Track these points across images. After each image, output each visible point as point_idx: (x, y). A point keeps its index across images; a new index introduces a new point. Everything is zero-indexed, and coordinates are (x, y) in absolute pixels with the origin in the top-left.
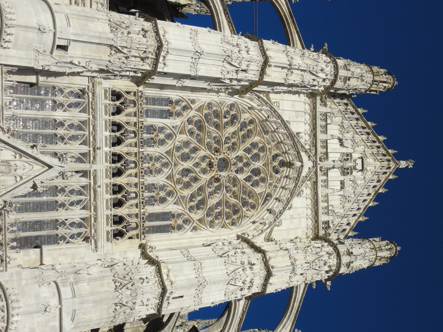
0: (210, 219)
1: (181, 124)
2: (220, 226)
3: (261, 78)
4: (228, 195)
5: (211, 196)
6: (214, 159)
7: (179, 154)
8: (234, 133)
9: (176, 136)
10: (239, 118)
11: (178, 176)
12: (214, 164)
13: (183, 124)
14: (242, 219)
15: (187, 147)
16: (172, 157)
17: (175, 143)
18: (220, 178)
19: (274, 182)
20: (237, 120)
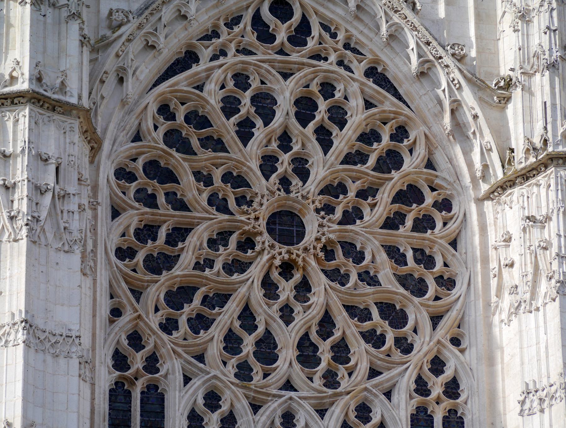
0: (432, 288)
1: (179, 355)
2: (453, 255)
3: (74, 112)
4: (366, 211)
5: (372, 274)
6: (273, 257)
7: (257, 368)
8: (197, 175)
9: (215, 377)
10: (155, 152)
11: (318, 382)
12: (286, 256)
13: (179, 350)
14: (437, 176)
15: (240, 341)
16: (268, 395)
17: (232, 383)
18: (323, 240)
19: (335, 46)
20: (160, 157)
